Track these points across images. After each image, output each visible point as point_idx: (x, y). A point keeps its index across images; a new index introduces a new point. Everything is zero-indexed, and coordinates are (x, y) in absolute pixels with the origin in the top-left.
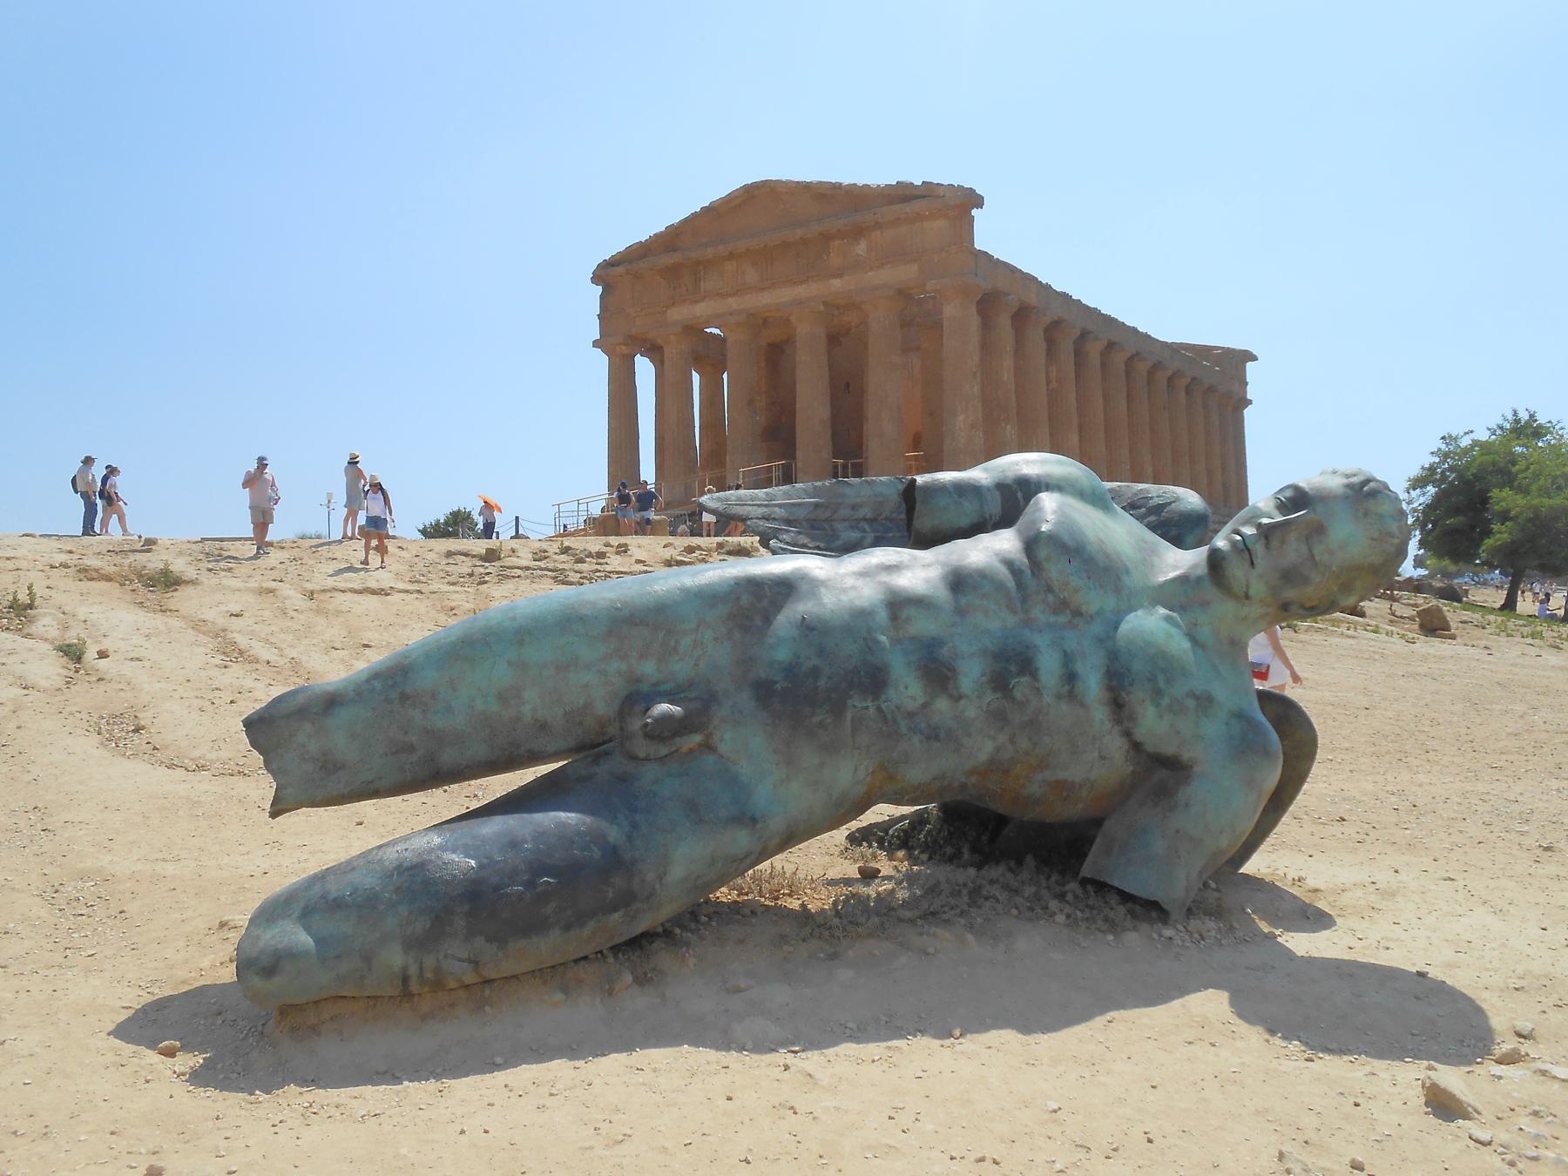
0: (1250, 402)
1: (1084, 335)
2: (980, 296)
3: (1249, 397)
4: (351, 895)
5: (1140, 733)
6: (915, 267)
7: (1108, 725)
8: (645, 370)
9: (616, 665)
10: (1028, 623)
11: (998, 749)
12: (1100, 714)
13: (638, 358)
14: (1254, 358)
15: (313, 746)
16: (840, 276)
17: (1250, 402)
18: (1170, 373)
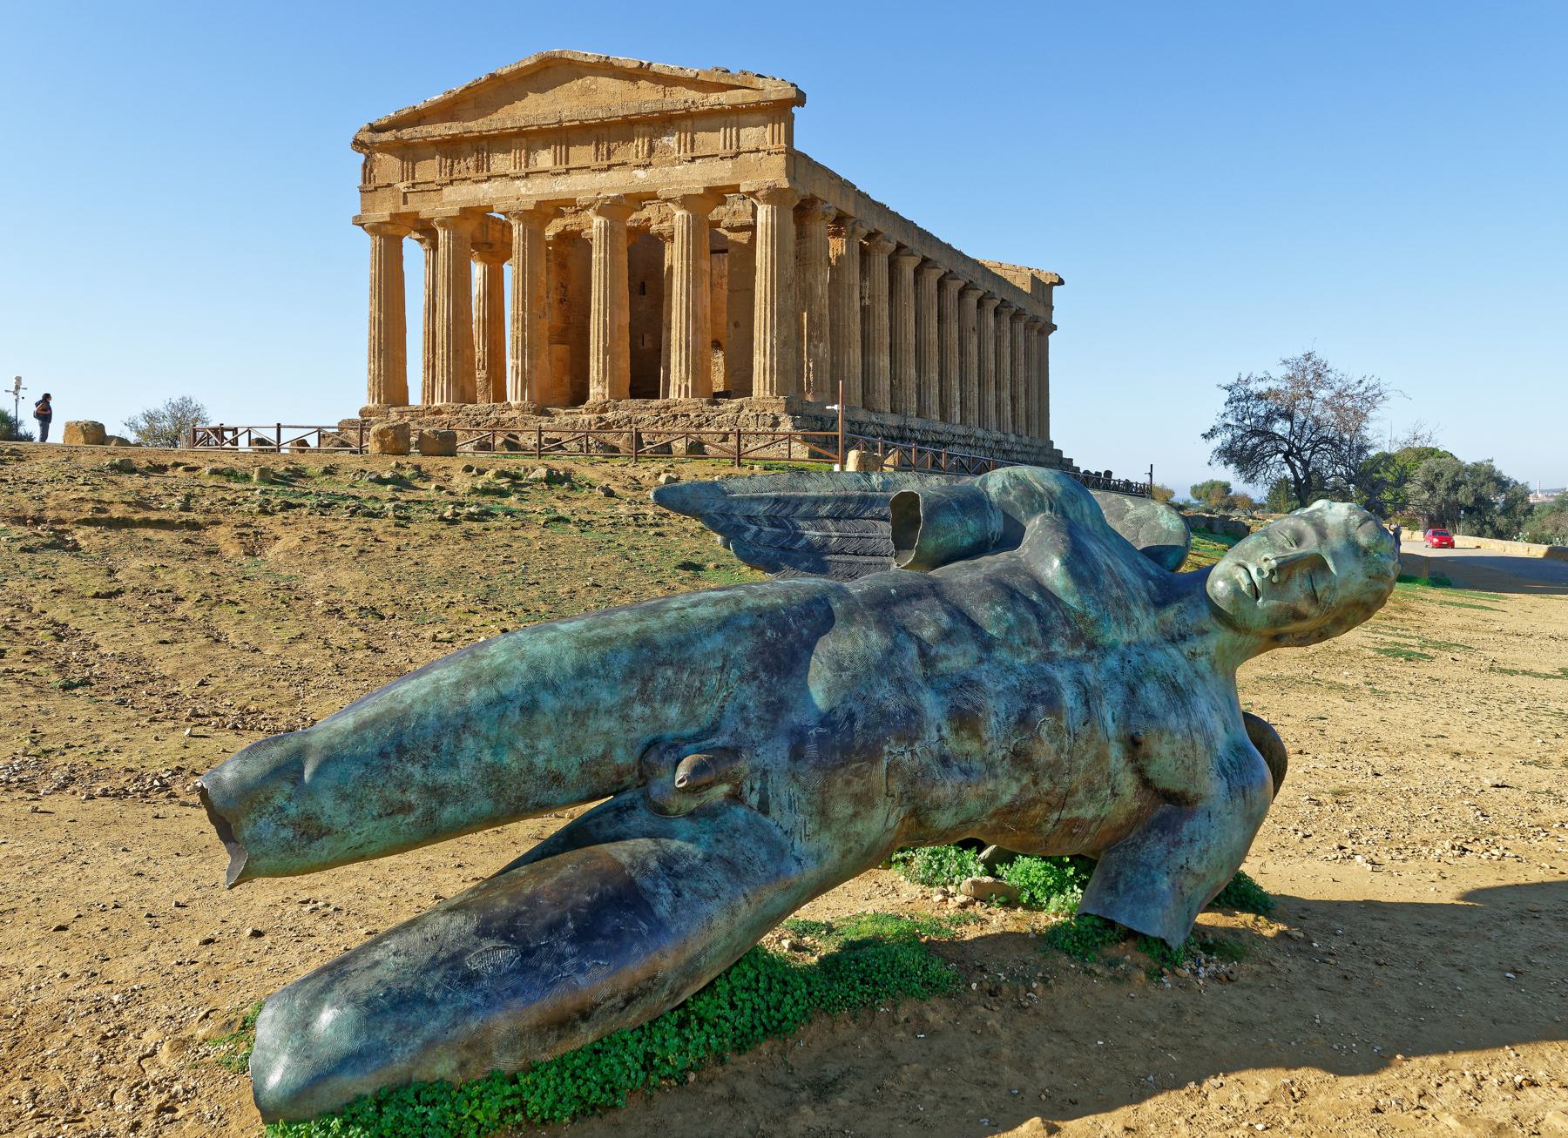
0: (1055, 328)
1: (988, 295)
2: (798, 202)
3: (1054, 322)
4: (385, 996)
5: (1153, 771)
6: (729, 164)
7: (1122, 763)
8: (413, 251)
9: (638, 710)
10: (1050, 658)
11: (1024, 789)
12: (1115, 753)
13: (406, 240)
14: (1061, 282)
15: (292, 811)
16: (646, 167)
17: (1055, 328)
18: (980, 293)
